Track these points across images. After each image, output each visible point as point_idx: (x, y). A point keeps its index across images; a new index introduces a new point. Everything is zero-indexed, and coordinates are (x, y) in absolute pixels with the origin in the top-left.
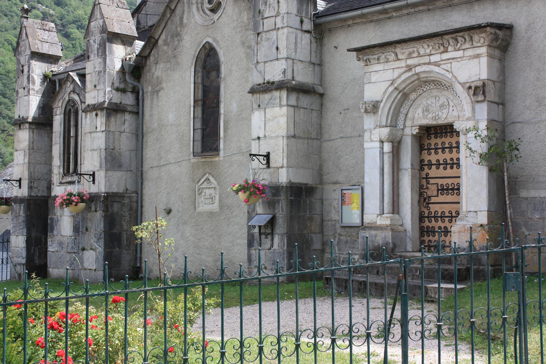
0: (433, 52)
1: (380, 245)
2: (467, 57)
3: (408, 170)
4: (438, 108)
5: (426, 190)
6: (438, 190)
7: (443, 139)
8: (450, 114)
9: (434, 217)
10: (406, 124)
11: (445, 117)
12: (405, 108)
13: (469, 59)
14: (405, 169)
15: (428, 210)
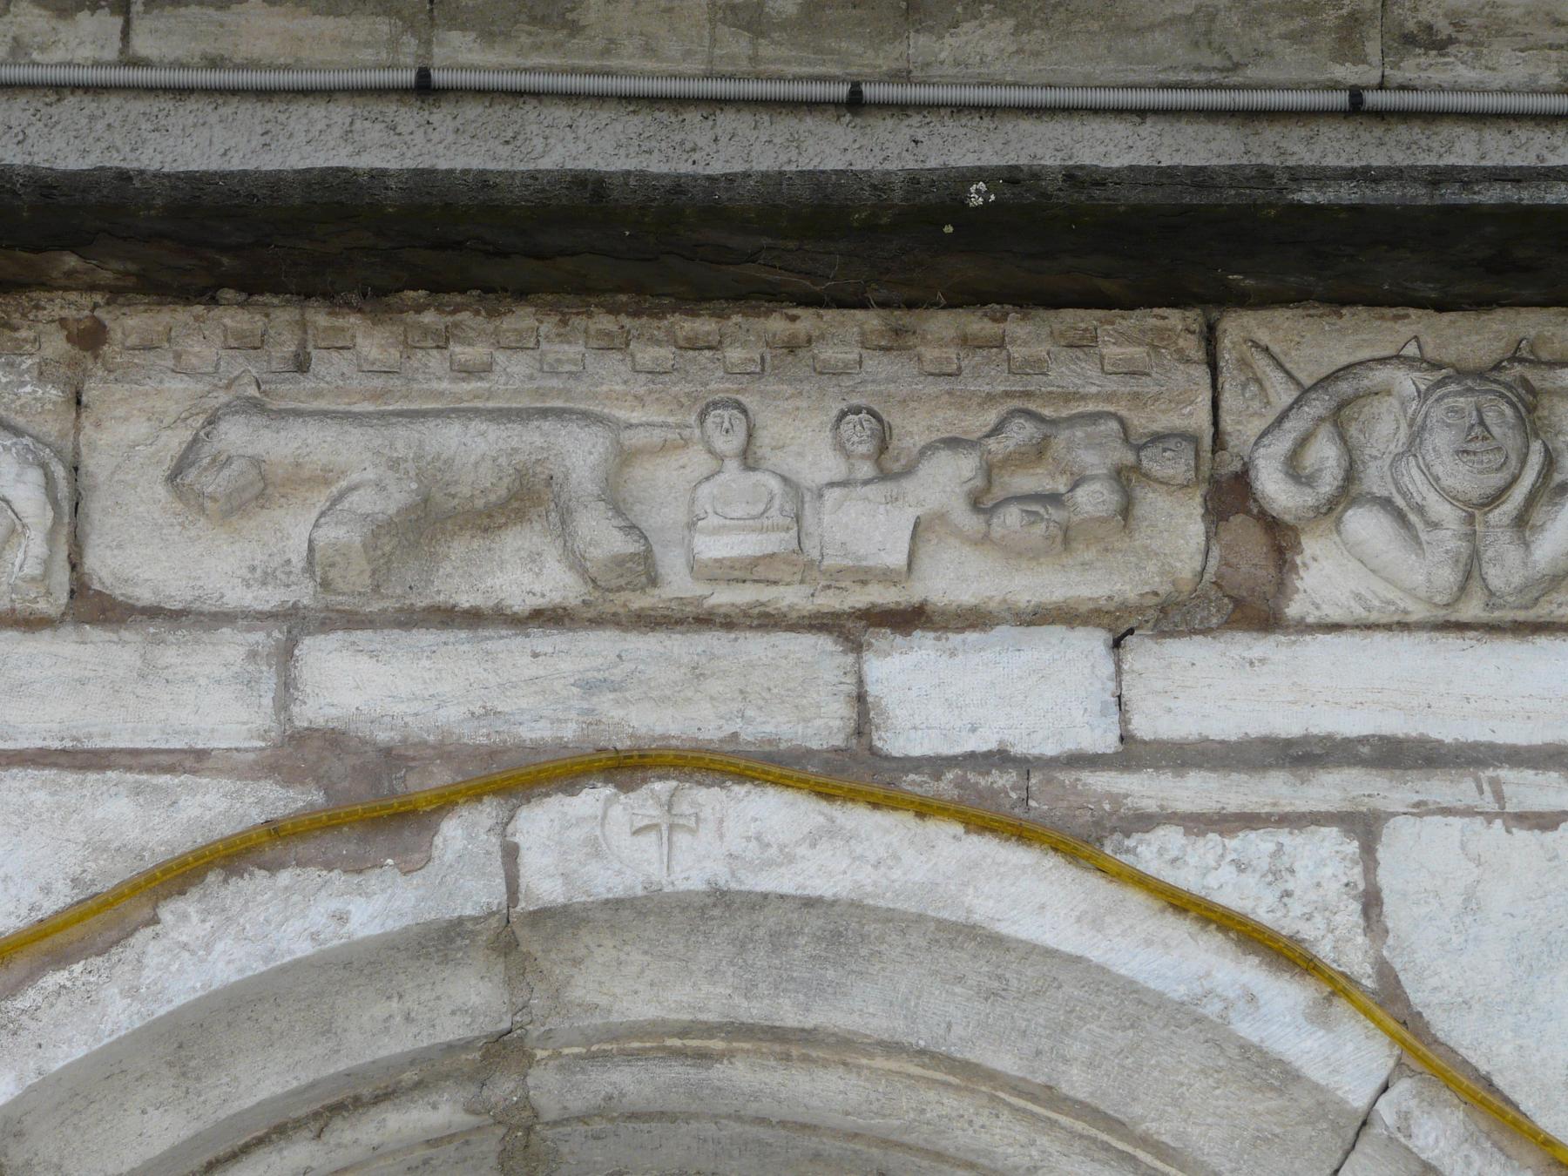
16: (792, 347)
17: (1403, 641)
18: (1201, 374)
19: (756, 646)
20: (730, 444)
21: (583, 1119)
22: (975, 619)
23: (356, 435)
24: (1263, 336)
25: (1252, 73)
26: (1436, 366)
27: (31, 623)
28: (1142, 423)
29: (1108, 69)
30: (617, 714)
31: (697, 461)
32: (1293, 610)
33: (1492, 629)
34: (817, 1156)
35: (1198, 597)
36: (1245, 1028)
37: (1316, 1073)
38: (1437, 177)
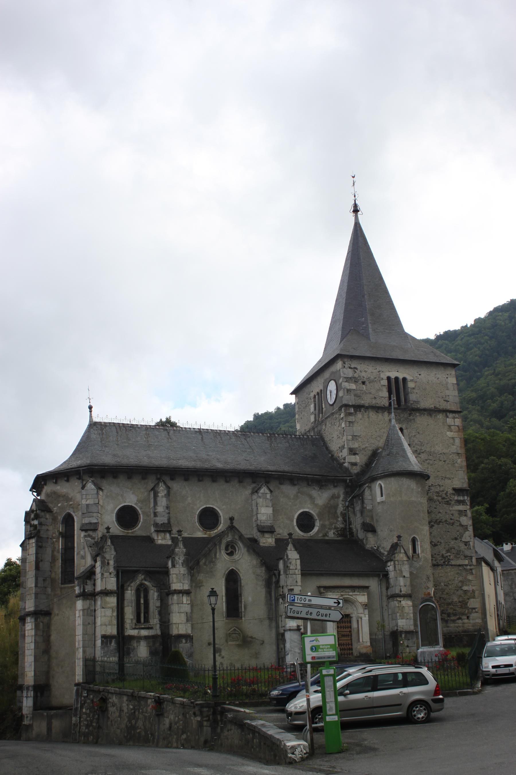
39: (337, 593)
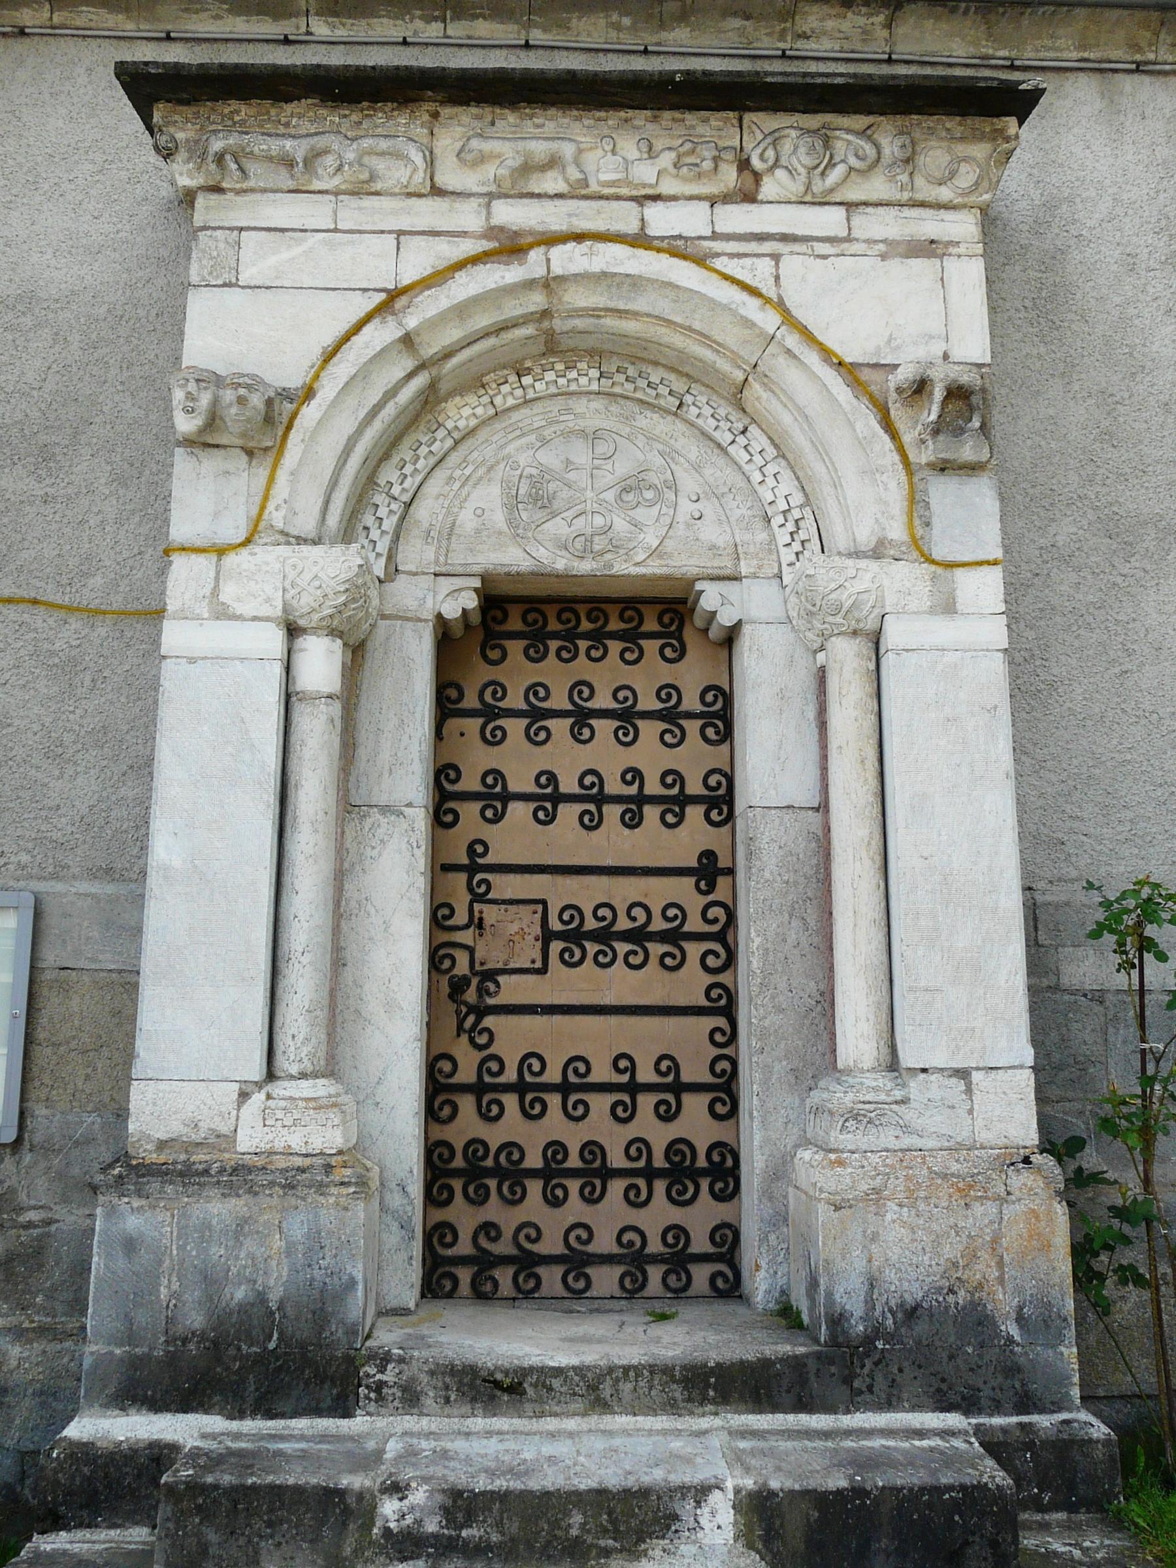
0: (668, 187)
1: (274, 1298)
2: (870, 242)
3: (407, 811)
4: (610, 496)
5: (466, 937)
6: (547, 937)
7: (582, 668)
8: (680, 530)
9: (520, 1088)
10: (400, 557)
11: (655, 544)
12: (408, 469)
13: (883, 257)
14: (386, 809)
15: (480, 1048)
16: (626, 121)
17: (789, 206)
18: (738, 130)
19: (615, 204)
20: (609, 148)
21: (567, 333)
22: (674, 198)
23: (507, 144)
24: (755, 120)
25: (755, 45)
26: (802, 129)
27: (420, 196)
28: (721, 144)
29: (715, 43)
30: (577, 223)
31: (600, 152)
32: (760, 198)
33: (814, 203)
34: (628, 344)
35: (735, 193)
36: (742, 311)
37: (760, 324)
38: (805, 75)
39: (428, 213)
